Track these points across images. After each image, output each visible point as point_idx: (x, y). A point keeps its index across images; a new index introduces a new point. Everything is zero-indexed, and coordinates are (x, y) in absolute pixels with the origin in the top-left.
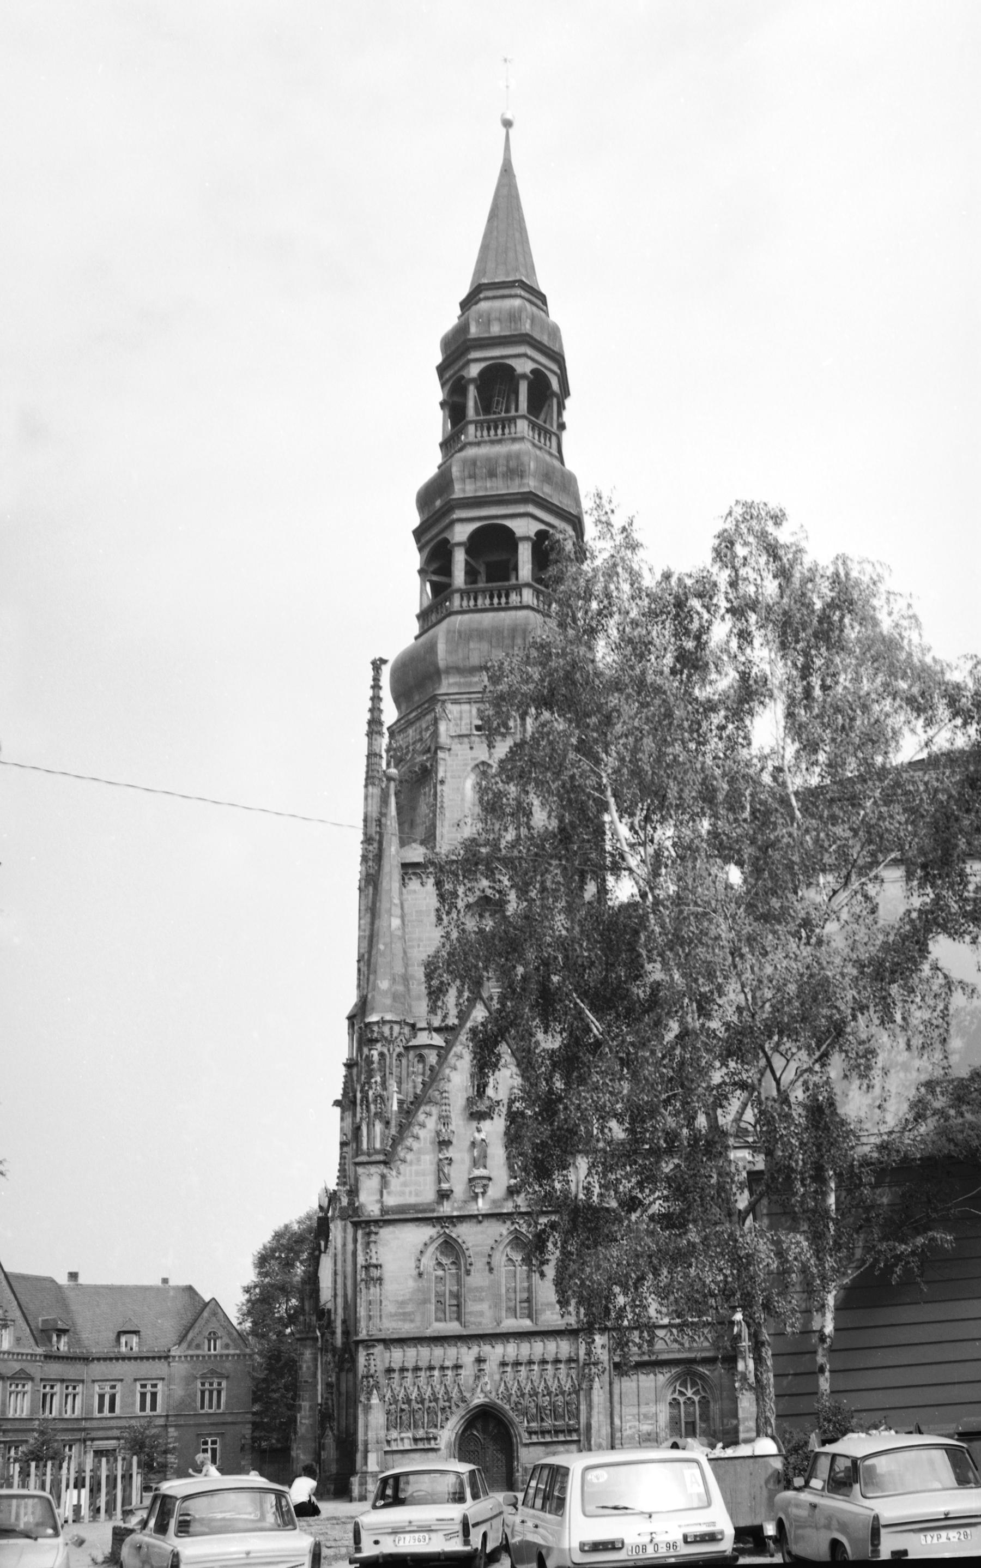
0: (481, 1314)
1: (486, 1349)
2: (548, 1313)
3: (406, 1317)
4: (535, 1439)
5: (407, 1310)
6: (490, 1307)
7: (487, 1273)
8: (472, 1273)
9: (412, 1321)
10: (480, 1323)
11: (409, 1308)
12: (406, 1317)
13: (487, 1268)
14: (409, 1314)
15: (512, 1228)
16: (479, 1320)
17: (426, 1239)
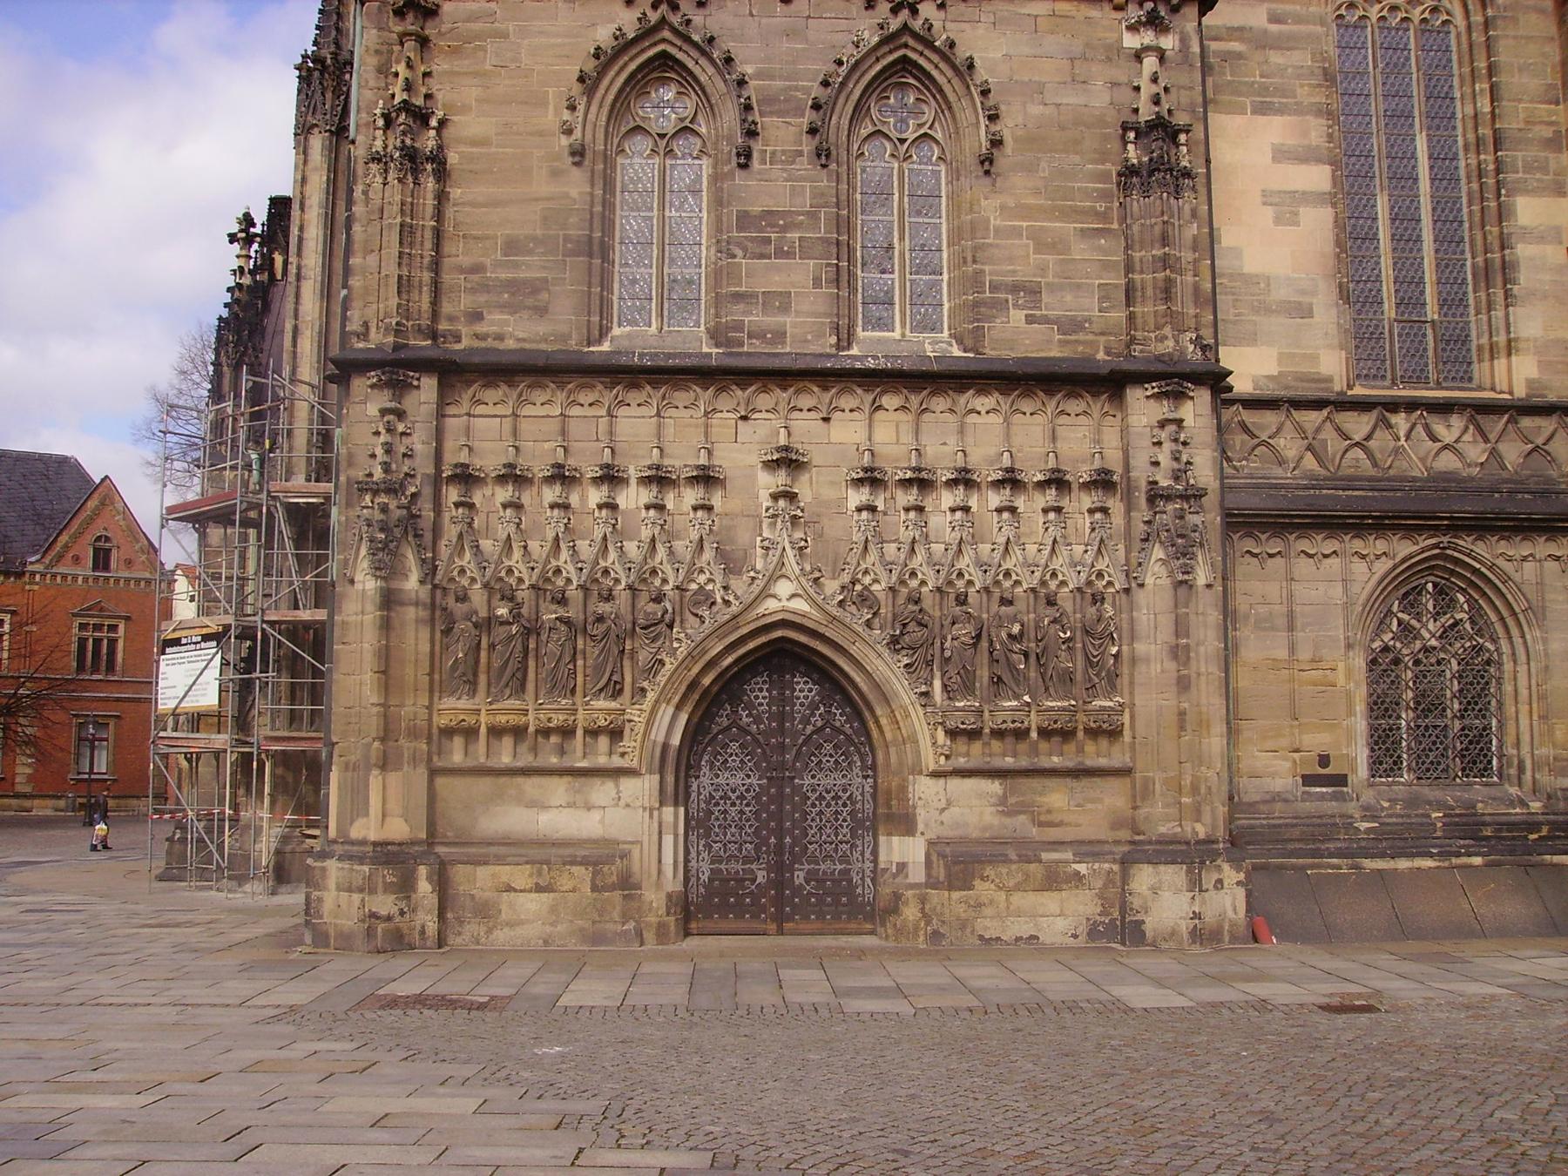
0: (783, 302)
1: (806, 429)
2: (1017, 316)
3: (526, 295)
4: (974, 755)
5: (523, 274)
6: (817, 282)
7: (804, 165)
8: (756, 163)
9: (542, 311)
10: (780, 336)
11: (531, 268)
12: (526, 295)
13: (808, 145)
14: (535, 287)
15: (895, 24)
16: (772, 320)
17: (603, 36)
